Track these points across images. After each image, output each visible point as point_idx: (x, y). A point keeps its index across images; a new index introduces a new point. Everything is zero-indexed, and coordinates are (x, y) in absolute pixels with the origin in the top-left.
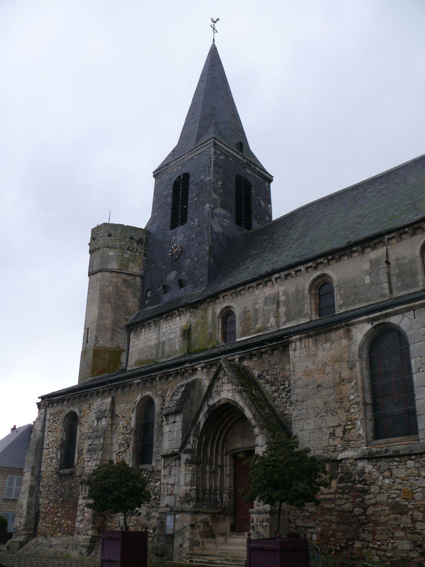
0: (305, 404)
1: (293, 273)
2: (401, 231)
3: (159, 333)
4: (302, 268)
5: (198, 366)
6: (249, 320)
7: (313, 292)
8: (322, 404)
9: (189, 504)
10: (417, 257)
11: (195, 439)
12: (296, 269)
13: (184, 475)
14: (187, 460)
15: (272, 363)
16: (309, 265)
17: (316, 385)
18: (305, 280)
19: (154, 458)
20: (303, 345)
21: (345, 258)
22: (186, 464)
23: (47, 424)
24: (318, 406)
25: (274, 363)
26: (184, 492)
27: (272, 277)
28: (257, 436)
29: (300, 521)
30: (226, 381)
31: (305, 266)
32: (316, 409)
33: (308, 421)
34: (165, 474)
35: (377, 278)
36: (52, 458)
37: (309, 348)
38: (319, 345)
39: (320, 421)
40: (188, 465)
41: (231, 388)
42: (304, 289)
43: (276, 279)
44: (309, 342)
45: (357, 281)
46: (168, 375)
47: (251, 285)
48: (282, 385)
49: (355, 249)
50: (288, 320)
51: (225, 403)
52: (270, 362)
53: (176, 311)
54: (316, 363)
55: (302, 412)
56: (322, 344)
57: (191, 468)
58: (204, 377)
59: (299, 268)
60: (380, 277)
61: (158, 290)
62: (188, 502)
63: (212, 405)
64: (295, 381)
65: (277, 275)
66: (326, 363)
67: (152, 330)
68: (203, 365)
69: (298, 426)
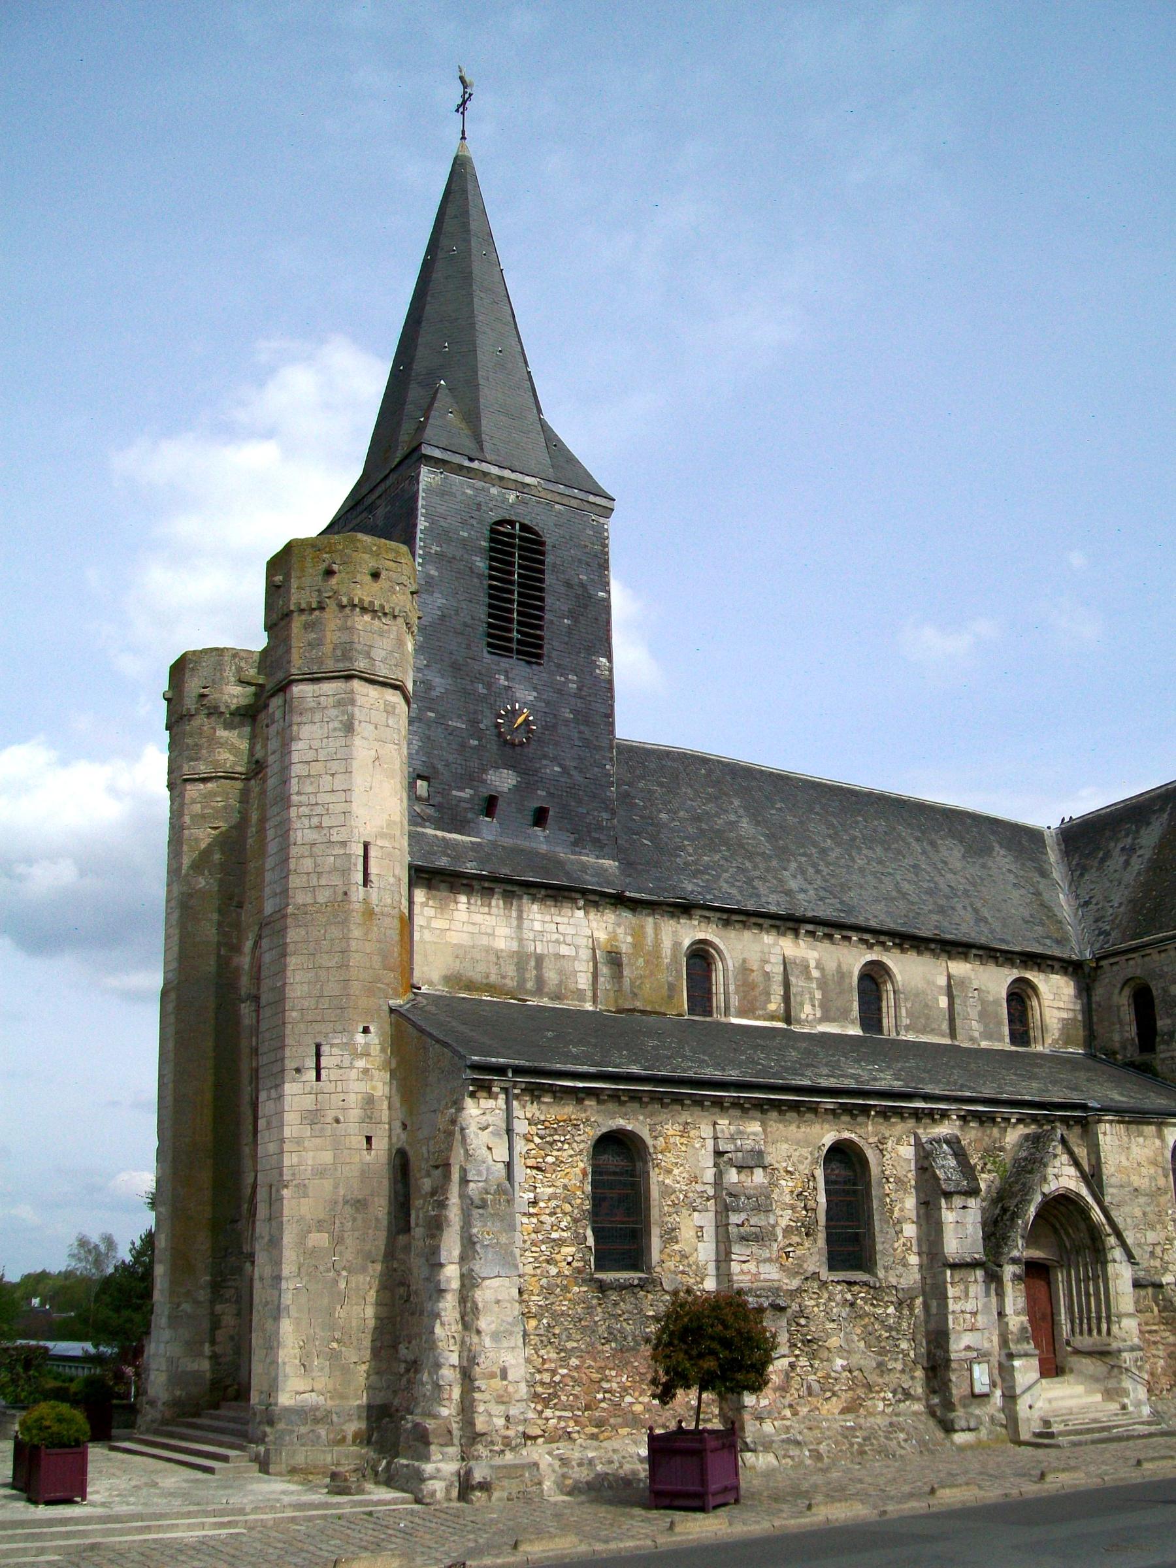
3: (520, 927)
6: (753, 989)
12: (845, 933)
14: (1015, 1275)
16: (866, 936)
17: (1131, 1188)
18: (854, 958)
19: (880, 1263)
22: (1013, 1281)
23: (520, 1146)
31: (860, 935)
34: (957, 1295)
36: (560, 1242)
42: (851, 973)
43: (807, 931)
46: (865, 1110)
47: (760, 921)
49: (933, 946)
50: (825, 1018)
53: (578, 896)
59: (849, 934)
61: (454, 793)
65: (810, 927)
67: (494, 910)
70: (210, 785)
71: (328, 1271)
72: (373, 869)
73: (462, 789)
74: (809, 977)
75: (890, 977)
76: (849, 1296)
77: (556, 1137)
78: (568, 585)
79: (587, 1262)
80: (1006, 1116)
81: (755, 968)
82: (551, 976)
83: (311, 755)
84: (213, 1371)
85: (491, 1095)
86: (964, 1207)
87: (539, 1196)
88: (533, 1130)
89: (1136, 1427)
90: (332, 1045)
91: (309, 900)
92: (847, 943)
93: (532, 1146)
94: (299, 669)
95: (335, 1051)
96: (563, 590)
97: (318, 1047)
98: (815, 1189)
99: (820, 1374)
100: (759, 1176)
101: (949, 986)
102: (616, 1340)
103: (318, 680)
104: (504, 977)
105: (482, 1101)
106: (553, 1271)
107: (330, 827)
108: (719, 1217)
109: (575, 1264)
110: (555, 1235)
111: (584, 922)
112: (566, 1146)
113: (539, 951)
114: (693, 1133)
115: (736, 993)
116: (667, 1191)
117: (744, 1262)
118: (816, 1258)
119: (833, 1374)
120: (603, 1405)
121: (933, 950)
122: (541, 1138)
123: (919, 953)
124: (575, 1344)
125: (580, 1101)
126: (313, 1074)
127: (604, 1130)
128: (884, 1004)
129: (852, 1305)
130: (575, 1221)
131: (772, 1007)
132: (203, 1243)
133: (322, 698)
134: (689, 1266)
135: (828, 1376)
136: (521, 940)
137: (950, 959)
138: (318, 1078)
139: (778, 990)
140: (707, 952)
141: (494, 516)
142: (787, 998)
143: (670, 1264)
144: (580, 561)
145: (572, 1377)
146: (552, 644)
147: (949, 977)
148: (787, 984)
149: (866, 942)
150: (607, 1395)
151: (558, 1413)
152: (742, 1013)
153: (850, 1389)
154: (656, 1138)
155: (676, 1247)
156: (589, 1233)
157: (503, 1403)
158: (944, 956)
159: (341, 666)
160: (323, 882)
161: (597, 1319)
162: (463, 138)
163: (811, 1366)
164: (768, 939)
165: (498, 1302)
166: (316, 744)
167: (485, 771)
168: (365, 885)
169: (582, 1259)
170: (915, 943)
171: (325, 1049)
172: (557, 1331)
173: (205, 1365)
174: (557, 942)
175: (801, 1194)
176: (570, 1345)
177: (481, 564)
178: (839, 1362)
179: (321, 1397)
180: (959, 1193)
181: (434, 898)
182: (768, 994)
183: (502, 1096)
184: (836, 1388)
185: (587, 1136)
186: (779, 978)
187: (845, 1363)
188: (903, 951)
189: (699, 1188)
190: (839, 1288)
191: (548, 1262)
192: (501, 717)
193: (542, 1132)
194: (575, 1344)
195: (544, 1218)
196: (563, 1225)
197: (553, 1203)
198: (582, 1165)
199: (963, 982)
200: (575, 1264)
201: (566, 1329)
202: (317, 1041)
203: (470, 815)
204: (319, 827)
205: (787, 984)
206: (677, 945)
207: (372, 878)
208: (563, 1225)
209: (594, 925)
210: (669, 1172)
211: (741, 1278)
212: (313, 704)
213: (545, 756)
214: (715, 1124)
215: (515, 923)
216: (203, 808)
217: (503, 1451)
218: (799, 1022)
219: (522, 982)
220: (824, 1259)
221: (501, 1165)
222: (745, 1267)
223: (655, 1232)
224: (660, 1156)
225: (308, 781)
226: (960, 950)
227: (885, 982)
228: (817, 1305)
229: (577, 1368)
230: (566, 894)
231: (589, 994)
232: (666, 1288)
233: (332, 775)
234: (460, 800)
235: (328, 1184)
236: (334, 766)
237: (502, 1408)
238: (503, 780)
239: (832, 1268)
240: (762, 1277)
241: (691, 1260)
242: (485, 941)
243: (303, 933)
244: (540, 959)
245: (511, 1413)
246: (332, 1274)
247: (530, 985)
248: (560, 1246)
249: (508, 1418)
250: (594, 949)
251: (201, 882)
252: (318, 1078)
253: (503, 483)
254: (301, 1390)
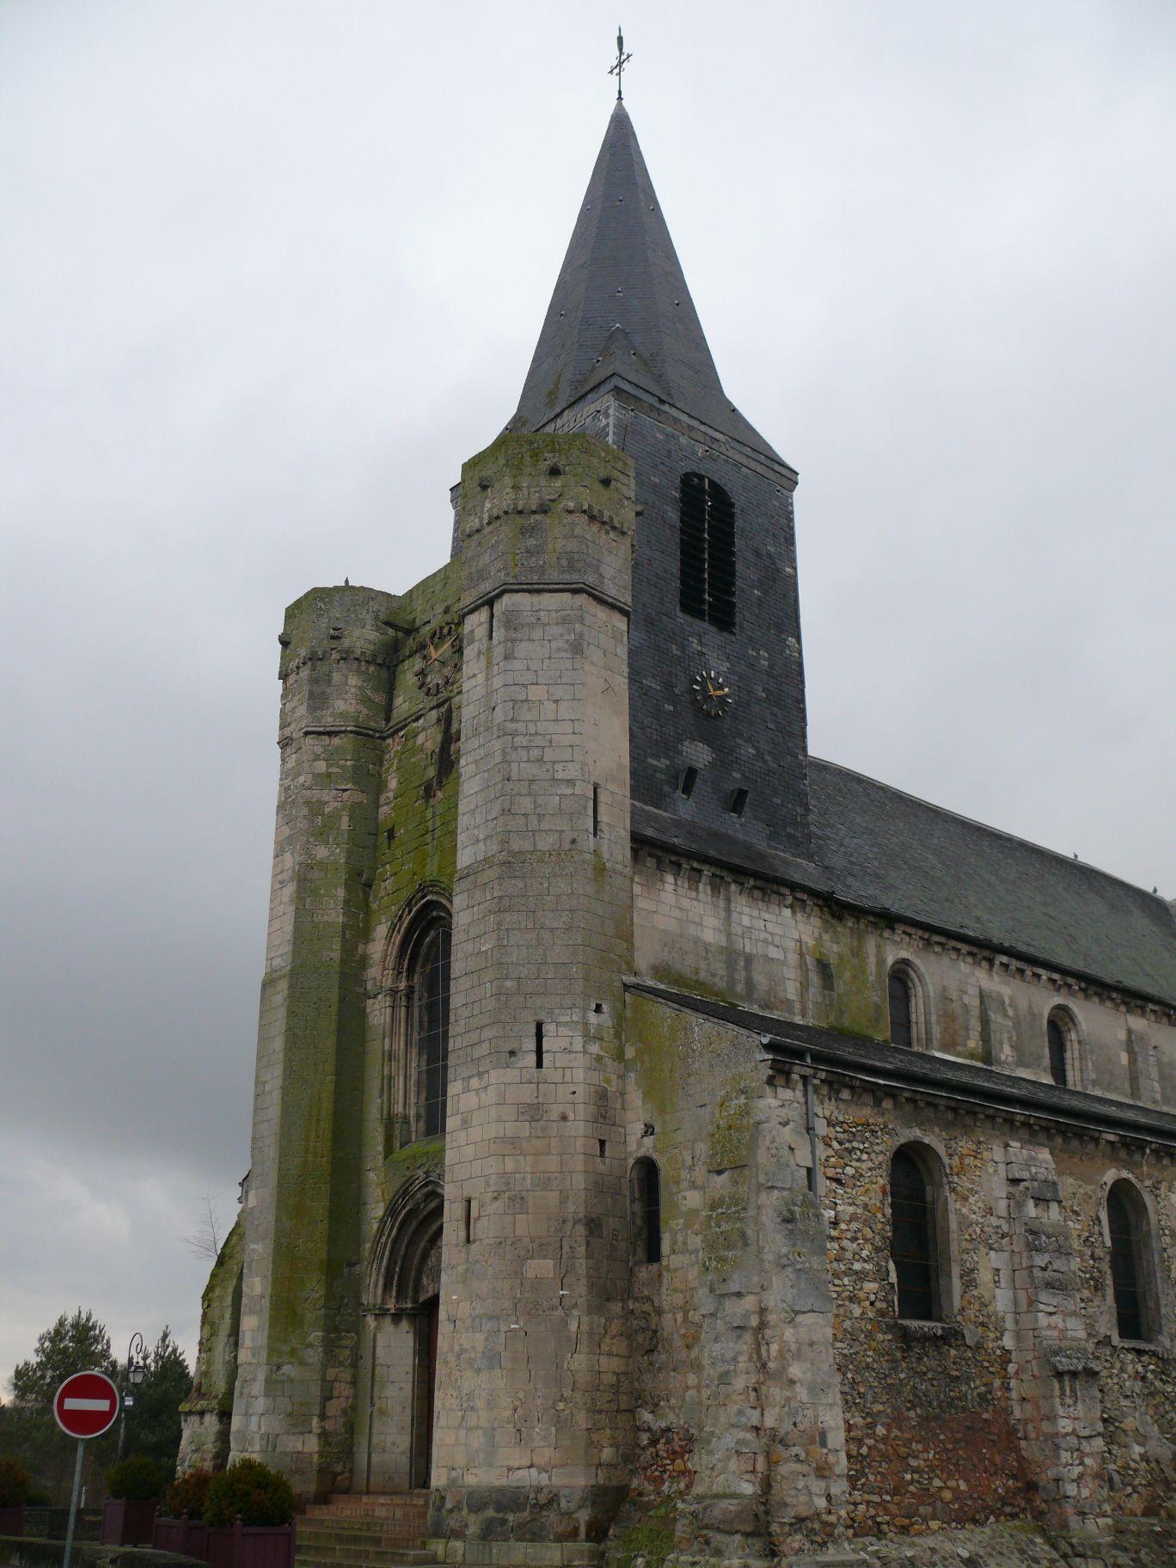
1: (1029, 973)
3: (728, 919)
18: (1045, 1000)
36: (861, 1276)
42: (1041, 1015)
47: (959, 945)
49: (1114, 995)
53: (787, 892)
59: (1040, 971)
65: (1004, 959)
67: (702, 896)
70: (336, 741)
71: (554, 1308)
72: (602, 817)
73: (657, 758)
74: (1005, 1015)
76: (1140, 1369)
77: (855, 1144)
78: (758, 555)
79: (890, 1303)
82: (760, 980)
83: (530, 677)
84: (321, 1454)
85: (788, 1084)
87: (841, 1216)
88: (831, 1132)
90: (558, 1024)
91: (528, 846)
93: (831, 1152)
94: (515, 577)
95: (563, 1031)
96: (752, 558)
97: (539, 1026)
98: (1101, 1234)
99: (1120, 1463)
100: (1054, 1212)
101: (1129, 1042)
102: (921, 1405)
103: (539, 591)
104: (714, 975)
105: (780, 1090)
106: (857, 1312)
107: (554, 762)
108: (1016, 1259)
109: (878, 1305)
110: (857, 1266)
111: (792, 923)
112: (865, 1157)
113: (747, 950)
114: (986, 1155)
115: (938, 1022)
116: (965, 1224)
117: (1051, 1314)
118: (1106, 1317)
119: (1132, 1464)
120: (912, 1488)
122: (840, 1143)
123: (1102, 1001)
124: (881, 1407)
125: (877, 1103)
126: (532, 1059)
127: (903, 1141)
128: (1068, 1055)
129: (1144, 1379)
130: (877, 1250)
131: (972, 1044)
132: (314, 1289)
133: (542, 613)
134: (989, 1317)
135: (1126, 1467)
136: (729, 935)
138: (539, 1064)
139: (975, 1025)
141: (686, 467)
142: (985, 1036)
143: (970, 1313)
144: (767, 531)
145: (879, 1451)
146: (744, 614)
147: (1130, 1032)
148: (985, 1021)
150: (916, 1476)
151: (867, 1497)
152: (945, 1048)
153: (1150, 1484)
154: (951, 1156)
155: (975, 1293)
156: (892, 1266)
157: (824, 1477)
158: (1123, 1008)
159: (567, 577)
160: (545, 826)
161: (902, 1376)
162: (620, 98)
163: (1110, 1452)
164: (964, 967)
165: (811, 1344)
166: (534, 665)
167: (681, 741)
168: (595, 834)
169: (885, 1300)
171: (548, 1028)
172: (862, 1390)
173: (312, 1445)
174: (765, 941)
175: (1087, 1240)
176: (878, 1407)
177: (673, 516)
178: (1138, 1449)
179: (545, 1476)
181: (641, 873)
182: (967, 1029)
183: (800, 1086)
184: (1136, 1482)
185: (886, 1146)
186: (975, 1012)
187: (1142, 1450)
188: (1087, 997)
189: (994, 1221)
190: (1130, 1357)
191: (851, 1299)
192: (697, 683)
193: (841, 1136)
194: (881, 1407)
195: (845, 1243)
196: (865, 1253)
197: (854, 1226)
198: (881, 1181)
199: (1142, 1038)
200: (878, 1305)
201: (871, 1387)
202: (539, 1017)
203: (666, 788)
204: (541, 760)
205: (985, 1021)
206: (881, 961)
207: (602, 826)
208: (865, 1253)
209: (801, 926)
210: (965, 1199)
211: (1049, 1333)
212: (529, 620)
213: (740, 735)
214: (1007, 1145)
215: (723, 914)
216: (328, 766)
217: (825, 1543)
218: (999, 1062)
219: (732, 982)
220: (1114, 1320)
221: (804, 1172)
222: (1053, 1319)
223: (956, 1271)
224: (956, 1179)
225: (526, 705)
228: (1111, 1377)
229: (885, 1440)
230: (775, 887)
231: (797, 1006)
232: (968, 1342)
233: (556, 702)
234: (656, 769)
235: (553, 1198)
236: (559, 692)
237: (823, 1484)
238: (699, 754)
239: (1122, 1336)
240: (1070, 1333)
241: (991, 1308)
242: (693, 930)
243: (521, 885)
244: (749, 959)
245: (833, 1491)
246: (560, 1312)
247: (740, 988)
248: (862, 1280)
249: (829, 1497)
250: (801, 955)
251: (322, 852)
252: (539, 1064)
253: (692, 434)
254: (516, 1464)
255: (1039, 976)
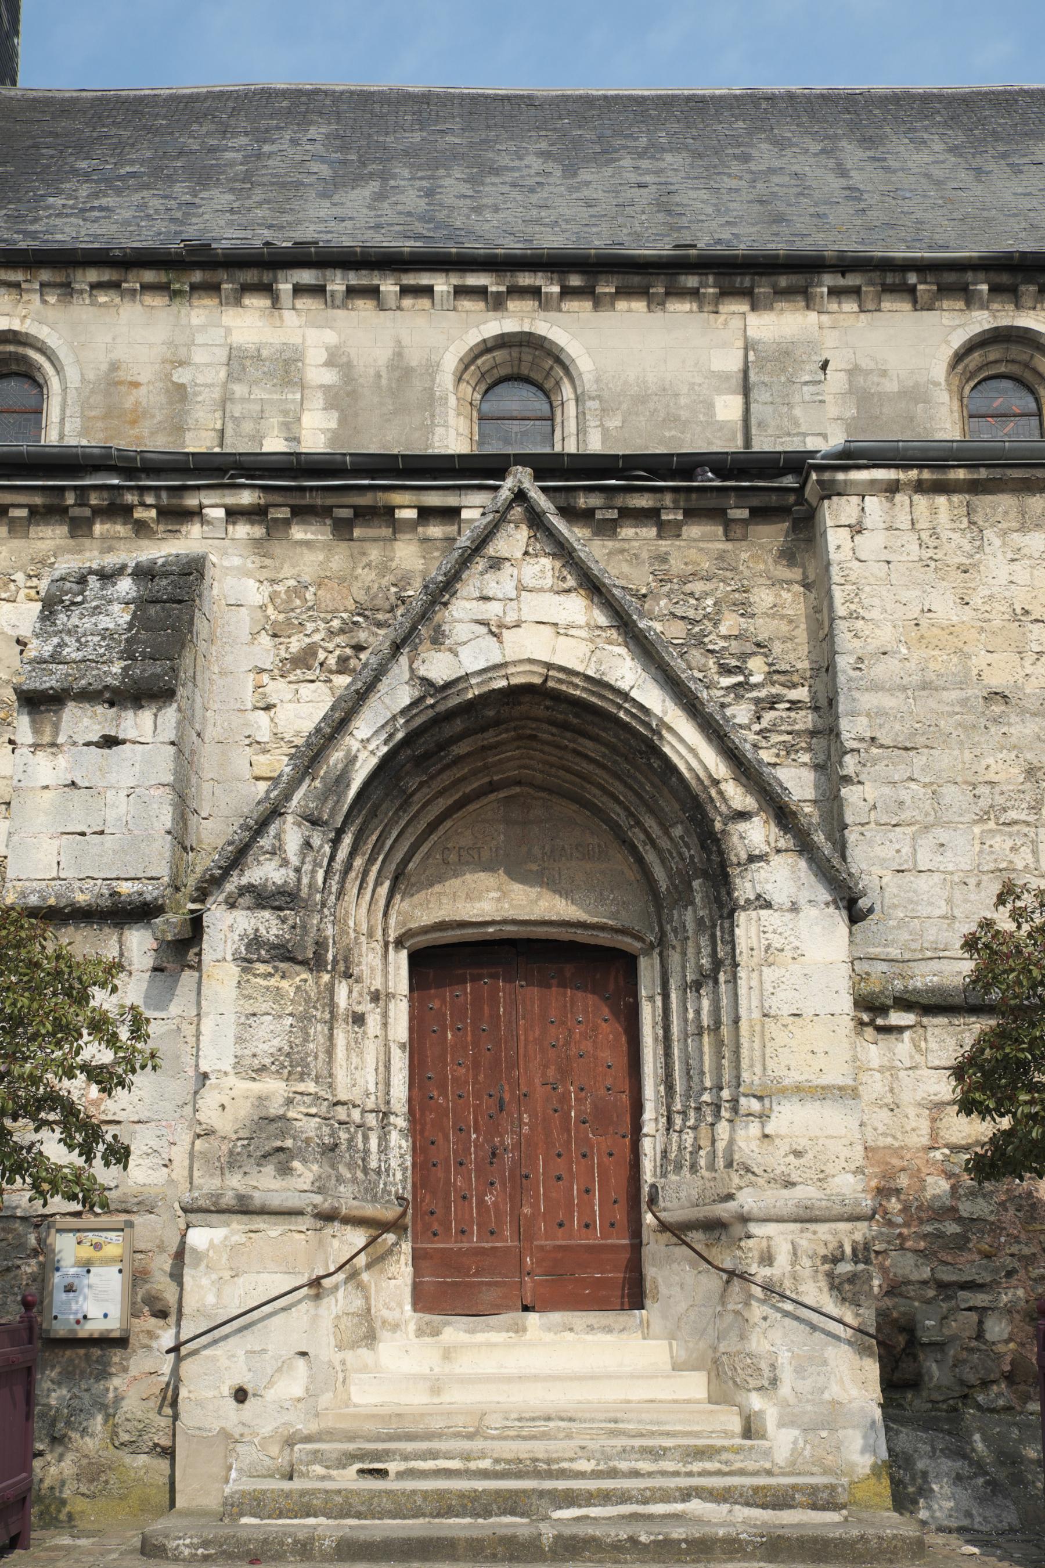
0: (919, 760)
2: (890, 279)
4: (442, 284)
5: (207, 498)
7: (466, 390)
8: (1016, 772)
9: (285, 1170)
10: (937, 384)
11: (316, 842)
12: (411, 279)
13: (230, 1018)
14: (255, 942)
15: (676, 565)
16: (474, 280)
17: (975, 692)
20: (903, 520)
21: (639, 305)
22: (246, 963)
24: (991, 776)
25: (690, 569)
26: (244, 1110)
27: (280, 274)
28: (752, 859)
29: (910, 1259)
30: (548, 582)
31: (455, 280)
32: (983, 790)
33: (942, 835)
35: (785, 409)
37: (934, 534)
38: (988, 533)
39: (1001, 843)
40: (261, 968)
41: (581, 620)
42: (432, 369)
44: (934, 511)
45: (683, 401)
48: (726, 670)
49: (691, 281)
51: (528, 689)
52: (663, 559)
54: (976, 601)
55: (904, 795)
56: (1004, 533)
57: (285, 984)
58: (237, 561)
59: (424, 279)
60: (797, 412)
62: (281, 1158)
63: (448, 685)
64: (860, 659)
65: (307, 276)
66: (1027, 612)
68: (246, 498)
69: (886, 852)
75: (558, 360)
80: (434, 499)
81: (143, 379)
86: (110, 742)
89: (695, 1506)
92: (424, 302)
121: (694, 294)
123: (655, 302)
137: (754, 308)
140: (25, 359)
147: (748, 346)
149: (481, 292)
170: (636, 280)
180: (88, 696)
188: (598, 303)
226: (783, 281)
227: (558, 384)
255: (428, 291)
